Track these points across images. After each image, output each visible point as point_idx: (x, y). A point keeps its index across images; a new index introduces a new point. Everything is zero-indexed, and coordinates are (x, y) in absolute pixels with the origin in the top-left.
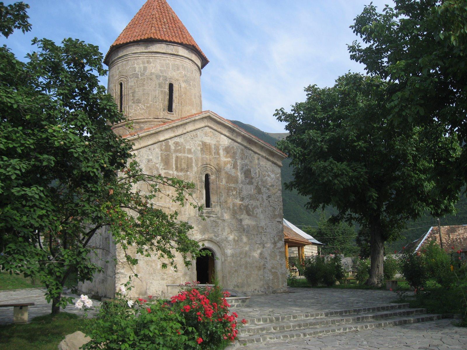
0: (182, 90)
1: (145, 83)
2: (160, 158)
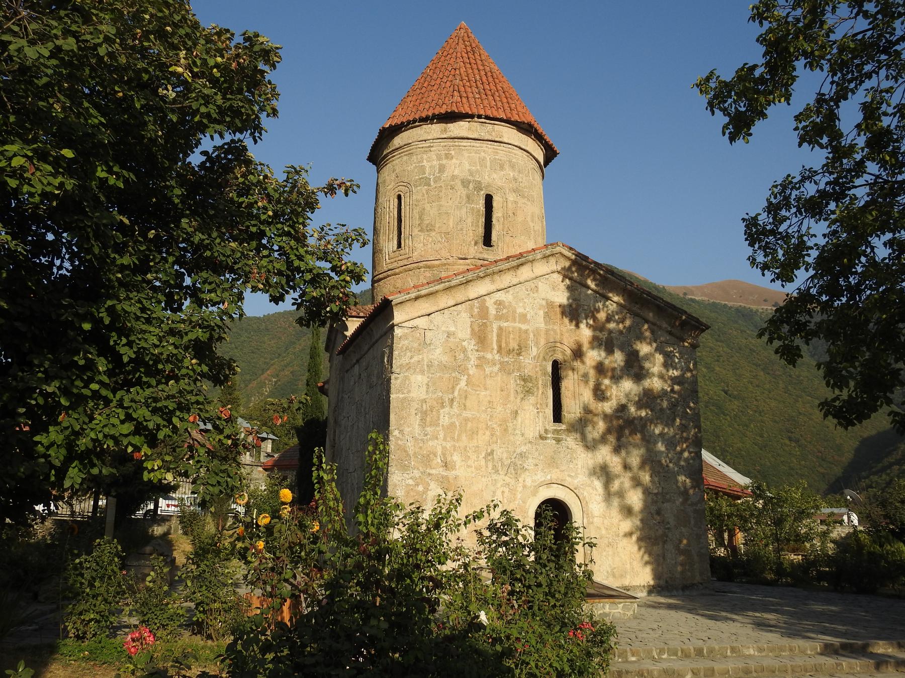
0: (510, 205)
2: (469, 330)
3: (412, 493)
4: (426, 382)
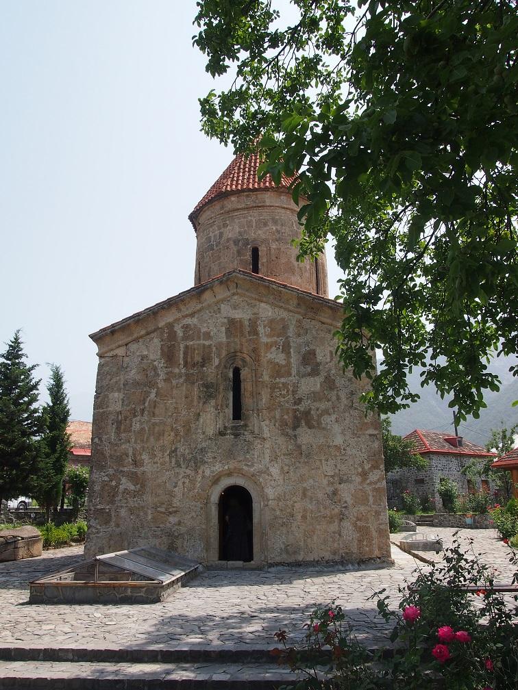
0: (273, 251)
1: (221, 254)
3: (107, 488)
4: (121, 397)
